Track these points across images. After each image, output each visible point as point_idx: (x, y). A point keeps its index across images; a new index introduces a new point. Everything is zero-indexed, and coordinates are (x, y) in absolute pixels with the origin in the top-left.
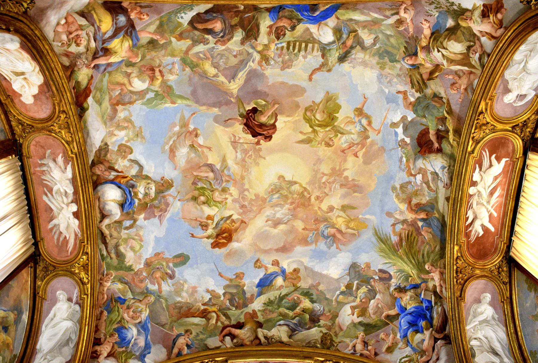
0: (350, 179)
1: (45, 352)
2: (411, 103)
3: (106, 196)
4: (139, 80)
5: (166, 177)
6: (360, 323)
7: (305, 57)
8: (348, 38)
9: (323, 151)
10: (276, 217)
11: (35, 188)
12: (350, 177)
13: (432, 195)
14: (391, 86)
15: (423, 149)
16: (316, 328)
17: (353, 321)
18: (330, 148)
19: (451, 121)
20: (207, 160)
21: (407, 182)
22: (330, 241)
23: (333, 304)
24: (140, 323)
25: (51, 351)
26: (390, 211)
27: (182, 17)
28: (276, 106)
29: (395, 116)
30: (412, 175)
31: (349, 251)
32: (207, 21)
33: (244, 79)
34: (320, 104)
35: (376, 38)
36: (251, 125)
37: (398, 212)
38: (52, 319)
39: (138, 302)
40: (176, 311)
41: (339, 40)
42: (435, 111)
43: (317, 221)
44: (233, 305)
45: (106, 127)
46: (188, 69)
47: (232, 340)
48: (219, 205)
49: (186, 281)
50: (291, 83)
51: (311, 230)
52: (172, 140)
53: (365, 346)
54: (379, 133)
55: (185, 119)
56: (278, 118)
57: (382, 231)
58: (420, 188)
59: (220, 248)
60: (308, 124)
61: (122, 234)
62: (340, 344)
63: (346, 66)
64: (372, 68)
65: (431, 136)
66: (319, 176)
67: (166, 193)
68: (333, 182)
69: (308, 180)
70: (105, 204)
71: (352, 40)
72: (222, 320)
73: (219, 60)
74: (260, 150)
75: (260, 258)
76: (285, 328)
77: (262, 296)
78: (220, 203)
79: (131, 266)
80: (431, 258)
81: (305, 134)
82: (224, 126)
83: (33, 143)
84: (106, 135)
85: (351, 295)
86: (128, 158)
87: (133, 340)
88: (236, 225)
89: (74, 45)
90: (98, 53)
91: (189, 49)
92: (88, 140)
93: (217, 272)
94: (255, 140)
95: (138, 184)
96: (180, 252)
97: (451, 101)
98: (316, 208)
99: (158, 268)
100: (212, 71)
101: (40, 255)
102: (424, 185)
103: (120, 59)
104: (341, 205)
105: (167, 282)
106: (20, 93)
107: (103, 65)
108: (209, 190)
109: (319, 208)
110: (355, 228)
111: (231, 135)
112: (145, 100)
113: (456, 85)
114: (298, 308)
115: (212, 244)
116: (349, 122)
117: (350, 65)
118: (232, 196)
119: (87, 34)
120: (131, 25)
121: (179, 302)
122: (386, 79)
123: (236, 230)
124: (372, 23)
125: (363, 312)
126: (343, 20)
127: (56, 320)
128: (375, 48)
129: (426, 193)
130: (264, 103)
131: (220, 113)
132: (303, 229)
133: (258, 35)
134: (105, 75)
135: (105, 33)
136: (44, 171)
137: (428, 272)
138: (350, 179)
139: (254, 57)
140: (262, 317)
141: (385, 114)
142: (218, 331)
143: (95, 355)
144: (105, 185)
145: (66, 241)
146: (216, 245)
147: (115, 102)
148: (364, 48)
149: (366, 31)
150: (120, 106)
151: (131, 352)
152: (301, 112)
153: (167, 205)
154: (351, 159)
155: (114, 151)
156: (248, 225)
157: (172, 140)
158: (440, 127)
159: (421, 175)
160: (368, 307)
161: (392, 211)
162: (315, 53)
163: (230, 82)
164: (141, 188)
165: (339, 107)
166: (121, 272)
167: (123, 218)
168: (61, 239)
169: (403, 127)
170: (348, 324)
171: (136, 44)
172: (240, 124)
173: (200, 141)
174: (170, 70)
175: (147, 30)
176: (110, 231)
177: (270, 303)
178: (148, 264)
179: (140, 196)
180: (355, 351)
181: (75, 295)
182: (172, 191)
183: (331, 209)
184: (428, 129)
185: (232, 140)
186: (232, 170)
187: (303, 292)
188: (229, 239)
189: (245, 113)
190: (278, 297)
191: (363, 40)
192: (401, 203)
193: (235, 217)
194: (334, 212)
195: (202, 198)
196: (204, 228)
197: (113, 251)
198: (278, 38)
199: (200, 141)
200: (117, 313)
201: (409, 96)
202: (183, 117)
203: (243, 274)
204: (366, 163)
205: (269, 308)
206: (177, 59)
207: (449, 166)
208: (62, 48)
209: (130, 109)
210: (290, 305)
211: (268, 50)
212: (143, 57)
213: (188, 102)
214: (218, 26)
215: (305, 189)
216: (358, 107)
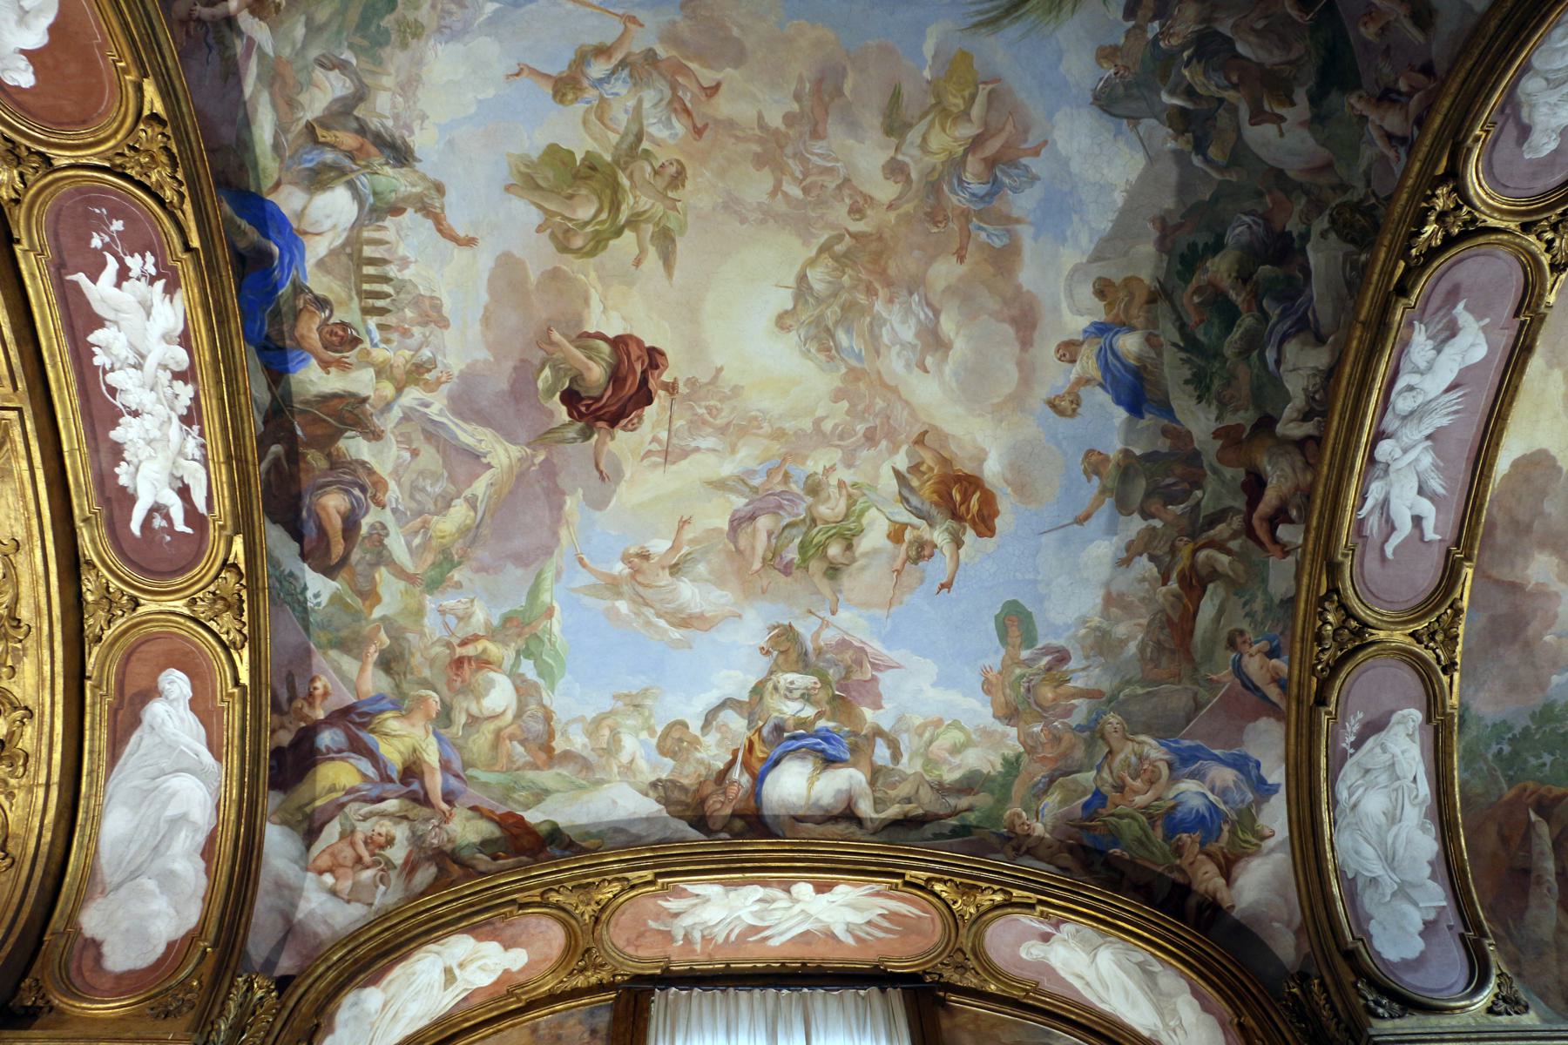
0: (795, 107)
1: (1160, 1025)
3: (794, 799)
4: (487, 695)
5: (762, 644)
6: (1315, 100)
7: (404, 263)
8: (333, 146)
9: (698, 194)
10: (916, 342)
11: (747, 956)
12: (787, 109)
16: (1309, 247)
17: (1302, 124)
18: (689, 172)
20: (718, 530)
22: (1010, 176)
23: (1234, 179)
24: (1170, 766)
25: (1161, 1014)
27: (316, 596)
28: (556, 336)
32: (322, 533)
33: (480, 429)
34: (546, 211)
35: (322, 66)
36: (613, 408)
38: (1088, 984)
39: (1112, 760)
40: (1164, 661)
41: (341, 172)
43: (935, 215)
44: (1187, 495)
45: (609, 782)
46: (456, 575)
47: (1290, 521)
48: (858, 507)
49: (1083, 621)
50: (485, 298)
51: (966, 235)
52: (655, 620)
53: (1394, 101)
54: (633, 20)
55: (595, 585)
56: (592, 331)
59: (996, 513)
60: (611, 243)
61: (909, 771)
62: (1374, 185)
63: (422, 141)
64: (419, 62)
66: (780, 206)
67: (810, 646)
68: (804, 161)
69: (796, 243)
70: (816, 804)
71: (338, 134)
72: (1226, 535)
73: (429, 495)
74: (692, 382)
75: (1045, 397)
76: (1291, 349)
77: (1174, 405)
78: (851, 501)
79: (1006, 760)
81: (643, 251)
82: (617, 483)
83: (630, 950)
84: (630, 784)
85: (1210, 117)
86: (698, 733)
87: (1212, 797)
88: (929, 459)
89: (389, 853)
90: (414, 792)
91: (401, 573)
92: (634, 830)
93: (1071, 528)
94: (661, 397)
95: (775, 714)
96: (992, 625)
98: (892, 217)
99: (1028, 690)
100: (459, 513)
101: (914, 978)
103: (432, 740)
105: (1073, 671)
106: (500, 973)
107: (445, 781)
108: (810, 529)
109: (890, 207)
110: (966, 93)
111: (646, 462)
112: (541, 682)
114: (1232, 294)
115: (980, 534)
116: (601, 119)
117: (416, 129)
118: (833, 468)
119: (365, 818)
120: (342, 716)
121: (1142, 649)
122: (451, 13)
123: (945, 462)
124: (277, 86)
125: (1275, 85)
126: (281, 170)
127: (1090, 975)
128: (354, 62)
130: (547, 372)
131: (580, 491)
132: (961, 259)
133: (352, 395)
134: (472, 777)
135: (365, 776)
136: (703, 937)
138: (795, 107)
139: (414, 404)
140: (1241, 413)
142: (1256, 554)
143: (1208, 912)
144: (764, 799)
145: (891, 916)
146: (985, 524)
147: (543, 756)
148: (360, 95)
149: (303, 98)
150: (554, 744)
151: (1239, 813)
152: (570, 264)
153: (844, 645)
154: (723, 107)
155: (675, 768)
156: (935, 428)
157: (655, 620)
160: (1260, 65)
162: (390, 235)
163: (489, 466)
164: (785, 709)
166: (1015, 788)
167: (864, 762)
168: (886, 924)
170: (1311, 142)
171: (393, 703)
172: (613, 438)
173: (660, 546)
174: (460, 619)
175: (354, 677)
176: (893, 801)
177: (1200, 384)
178: (1010, 715)
179: (809, 712)
180: (1403, 140)
181: (1036, 925)
182: (806, 629)
183: (895, 169)
185: (661, 460)
186: (753, 465)
187: (1179, 273)
188: (971, 483)
189: (580, 425)
190: (1183, 355)
191: (336, 101)
193: (902, 462)
194: (907, 159)
195: (834, 550)
196: (926, 552)
197: (952, 801)
198: (356, 341)
199: (660, 546)
200: (1126, 821)
202: (591, 590)
203: (1090, 453)
204: (739, 56)
205: (1216, 385)
206: (430, 602)
208: (393, 881)
209: (564, 721)
210: (1216, 321)
211: (391, 366)
212: (426, 684)
213: (549, 575)
214: (334, 503)
215: (823, 249)
216: (551, 92)
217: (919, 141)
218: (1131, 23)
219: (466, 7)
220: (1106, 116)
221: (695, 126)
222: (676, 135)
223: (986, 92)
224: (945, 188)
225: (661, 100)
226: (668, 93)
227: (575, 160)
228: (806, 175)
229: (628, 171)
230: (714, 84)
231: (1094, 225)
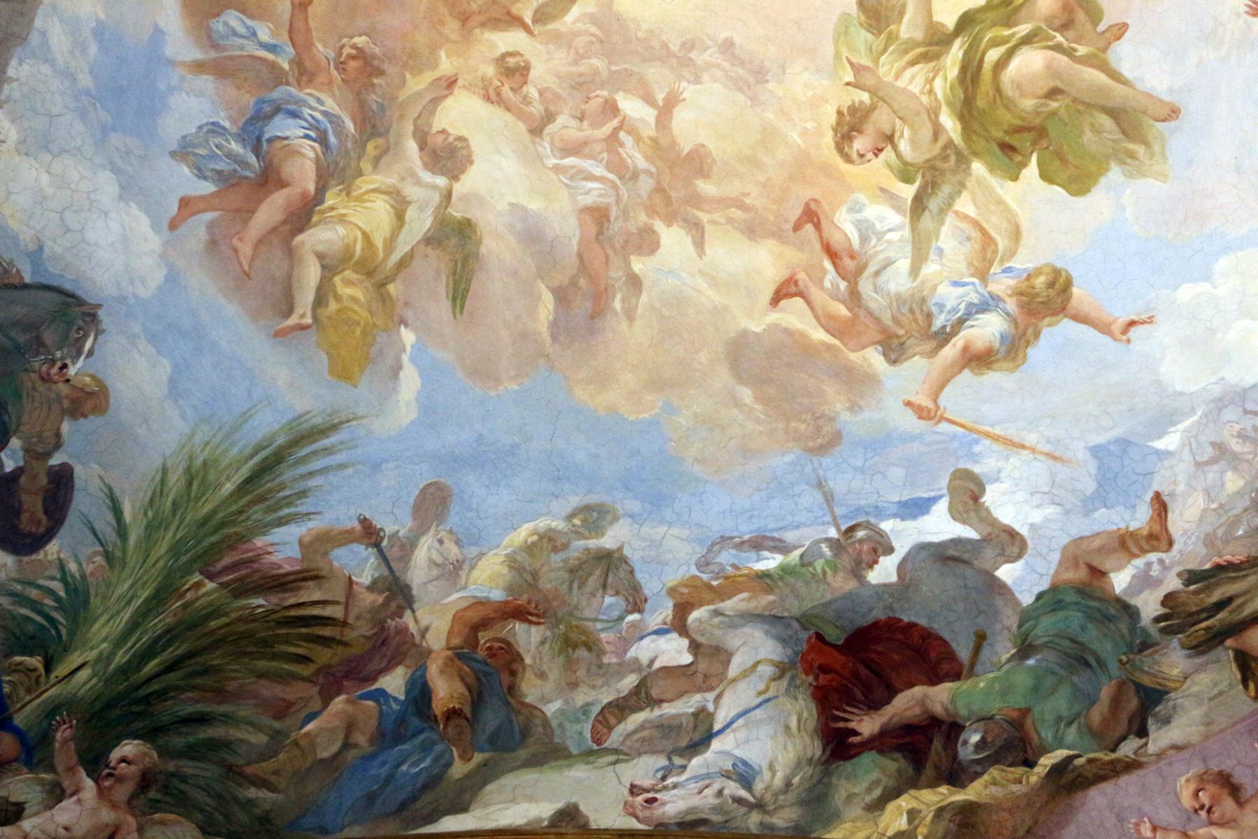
2: (1098, 573)
13: (571, 729)
14: (1198, 465)
15: (838, 660)
18: (828, 139)
19: (1015, 788)
21: (636, 588)
22: (230, 155)
26: (454, 509)
29: (1021, 496)
30: (682, 610)
31: (172, 279)
37: (453, 551)
42: (1060, 702)
51: (297, 33)
54: (923, 413)
57: (320, 472)
58: (610, 659)
65: (918, 690)
66: (659, 78)
68: (618, 166)
80: (189, 767)
97: (1128, 781)
98: (446, 64)
102: (630, 681)
104: (475, 214)
109: (451, 83)
110: (333, 306)
113: (1228, 805)
116: (987, 240)
129: (581, 697)
137: (94, 762)
141: (1031, 439)
158: (975, 738)
159: (687, 659)
161: (455, 517)
165: (1079, 183)
169: (957, 542)
184: (956, 676)
192: (512, 562)
194: (427, 177)
201: (1139, 562)
207: (759, 806)
216: (1076, 291)
217: (410, 214)
218: (55, 460)
219: (1213, 444)
220: (68, 286)
221: (818, 226)
222: (851, 210)
223: (299, 311)
224: (350, 125)
225: (877, 274)
226: (865, 286)
227: (1040, 165)
228: (613, 138)
229: (941, 143)
230: (783, 303)
231: (46, 69)
